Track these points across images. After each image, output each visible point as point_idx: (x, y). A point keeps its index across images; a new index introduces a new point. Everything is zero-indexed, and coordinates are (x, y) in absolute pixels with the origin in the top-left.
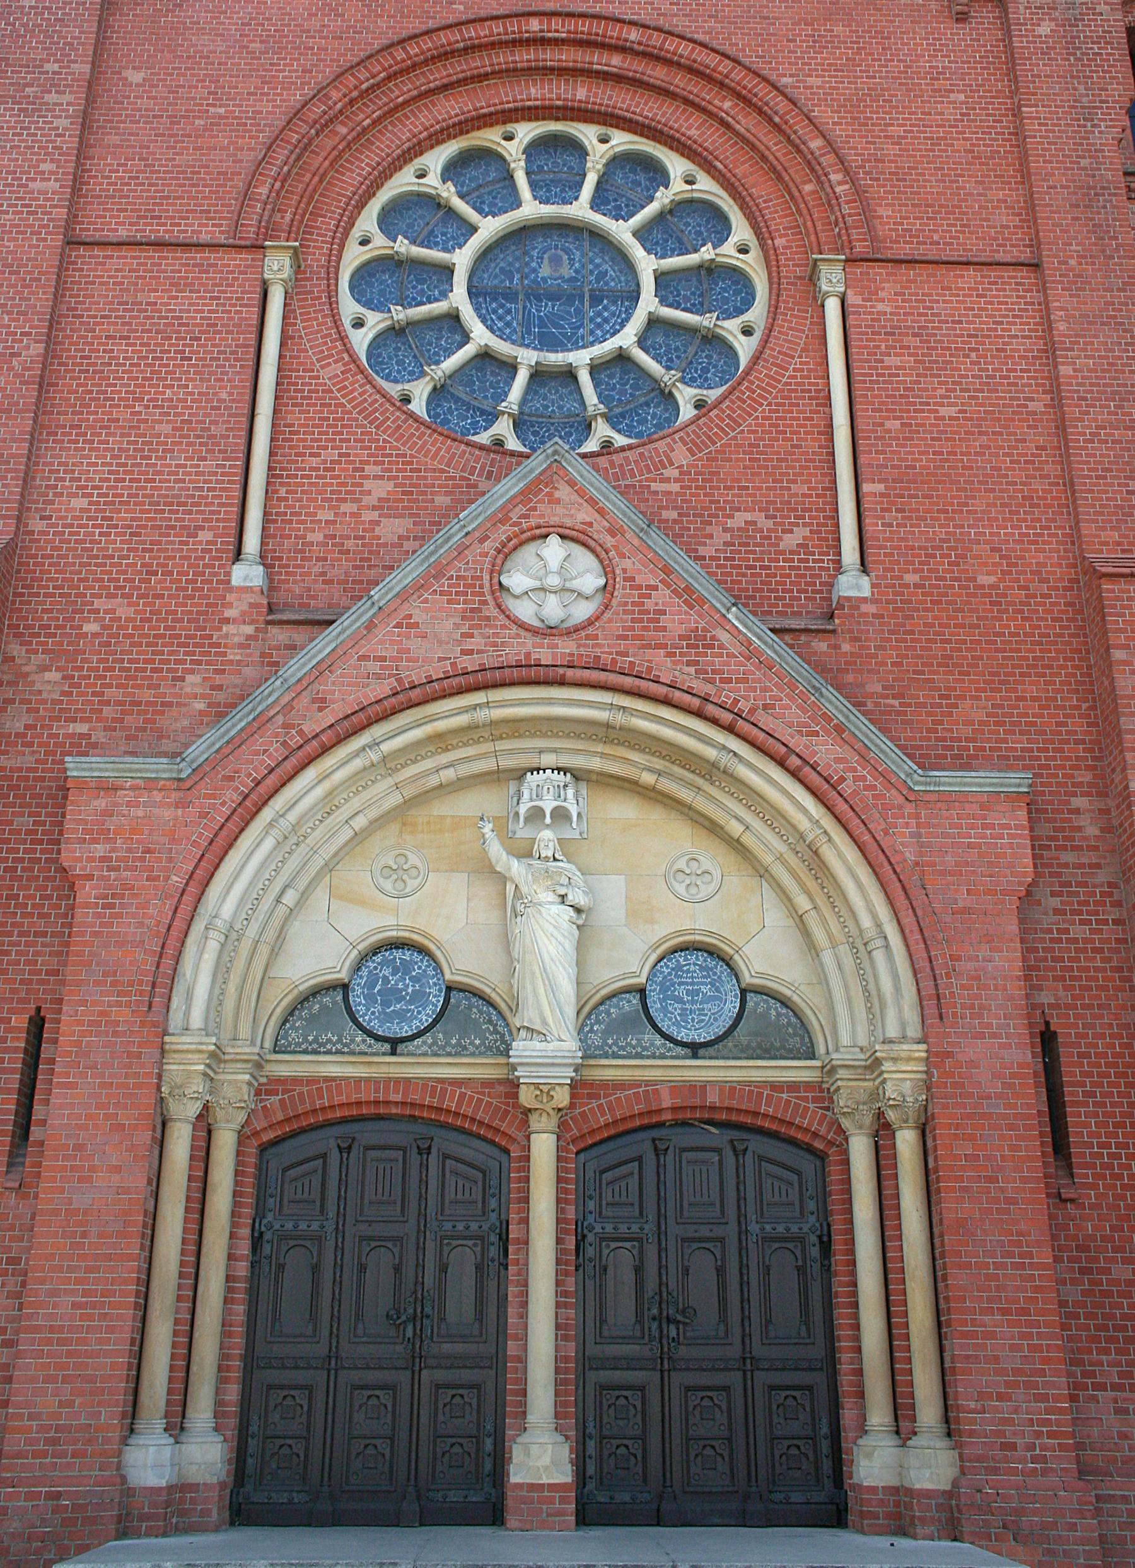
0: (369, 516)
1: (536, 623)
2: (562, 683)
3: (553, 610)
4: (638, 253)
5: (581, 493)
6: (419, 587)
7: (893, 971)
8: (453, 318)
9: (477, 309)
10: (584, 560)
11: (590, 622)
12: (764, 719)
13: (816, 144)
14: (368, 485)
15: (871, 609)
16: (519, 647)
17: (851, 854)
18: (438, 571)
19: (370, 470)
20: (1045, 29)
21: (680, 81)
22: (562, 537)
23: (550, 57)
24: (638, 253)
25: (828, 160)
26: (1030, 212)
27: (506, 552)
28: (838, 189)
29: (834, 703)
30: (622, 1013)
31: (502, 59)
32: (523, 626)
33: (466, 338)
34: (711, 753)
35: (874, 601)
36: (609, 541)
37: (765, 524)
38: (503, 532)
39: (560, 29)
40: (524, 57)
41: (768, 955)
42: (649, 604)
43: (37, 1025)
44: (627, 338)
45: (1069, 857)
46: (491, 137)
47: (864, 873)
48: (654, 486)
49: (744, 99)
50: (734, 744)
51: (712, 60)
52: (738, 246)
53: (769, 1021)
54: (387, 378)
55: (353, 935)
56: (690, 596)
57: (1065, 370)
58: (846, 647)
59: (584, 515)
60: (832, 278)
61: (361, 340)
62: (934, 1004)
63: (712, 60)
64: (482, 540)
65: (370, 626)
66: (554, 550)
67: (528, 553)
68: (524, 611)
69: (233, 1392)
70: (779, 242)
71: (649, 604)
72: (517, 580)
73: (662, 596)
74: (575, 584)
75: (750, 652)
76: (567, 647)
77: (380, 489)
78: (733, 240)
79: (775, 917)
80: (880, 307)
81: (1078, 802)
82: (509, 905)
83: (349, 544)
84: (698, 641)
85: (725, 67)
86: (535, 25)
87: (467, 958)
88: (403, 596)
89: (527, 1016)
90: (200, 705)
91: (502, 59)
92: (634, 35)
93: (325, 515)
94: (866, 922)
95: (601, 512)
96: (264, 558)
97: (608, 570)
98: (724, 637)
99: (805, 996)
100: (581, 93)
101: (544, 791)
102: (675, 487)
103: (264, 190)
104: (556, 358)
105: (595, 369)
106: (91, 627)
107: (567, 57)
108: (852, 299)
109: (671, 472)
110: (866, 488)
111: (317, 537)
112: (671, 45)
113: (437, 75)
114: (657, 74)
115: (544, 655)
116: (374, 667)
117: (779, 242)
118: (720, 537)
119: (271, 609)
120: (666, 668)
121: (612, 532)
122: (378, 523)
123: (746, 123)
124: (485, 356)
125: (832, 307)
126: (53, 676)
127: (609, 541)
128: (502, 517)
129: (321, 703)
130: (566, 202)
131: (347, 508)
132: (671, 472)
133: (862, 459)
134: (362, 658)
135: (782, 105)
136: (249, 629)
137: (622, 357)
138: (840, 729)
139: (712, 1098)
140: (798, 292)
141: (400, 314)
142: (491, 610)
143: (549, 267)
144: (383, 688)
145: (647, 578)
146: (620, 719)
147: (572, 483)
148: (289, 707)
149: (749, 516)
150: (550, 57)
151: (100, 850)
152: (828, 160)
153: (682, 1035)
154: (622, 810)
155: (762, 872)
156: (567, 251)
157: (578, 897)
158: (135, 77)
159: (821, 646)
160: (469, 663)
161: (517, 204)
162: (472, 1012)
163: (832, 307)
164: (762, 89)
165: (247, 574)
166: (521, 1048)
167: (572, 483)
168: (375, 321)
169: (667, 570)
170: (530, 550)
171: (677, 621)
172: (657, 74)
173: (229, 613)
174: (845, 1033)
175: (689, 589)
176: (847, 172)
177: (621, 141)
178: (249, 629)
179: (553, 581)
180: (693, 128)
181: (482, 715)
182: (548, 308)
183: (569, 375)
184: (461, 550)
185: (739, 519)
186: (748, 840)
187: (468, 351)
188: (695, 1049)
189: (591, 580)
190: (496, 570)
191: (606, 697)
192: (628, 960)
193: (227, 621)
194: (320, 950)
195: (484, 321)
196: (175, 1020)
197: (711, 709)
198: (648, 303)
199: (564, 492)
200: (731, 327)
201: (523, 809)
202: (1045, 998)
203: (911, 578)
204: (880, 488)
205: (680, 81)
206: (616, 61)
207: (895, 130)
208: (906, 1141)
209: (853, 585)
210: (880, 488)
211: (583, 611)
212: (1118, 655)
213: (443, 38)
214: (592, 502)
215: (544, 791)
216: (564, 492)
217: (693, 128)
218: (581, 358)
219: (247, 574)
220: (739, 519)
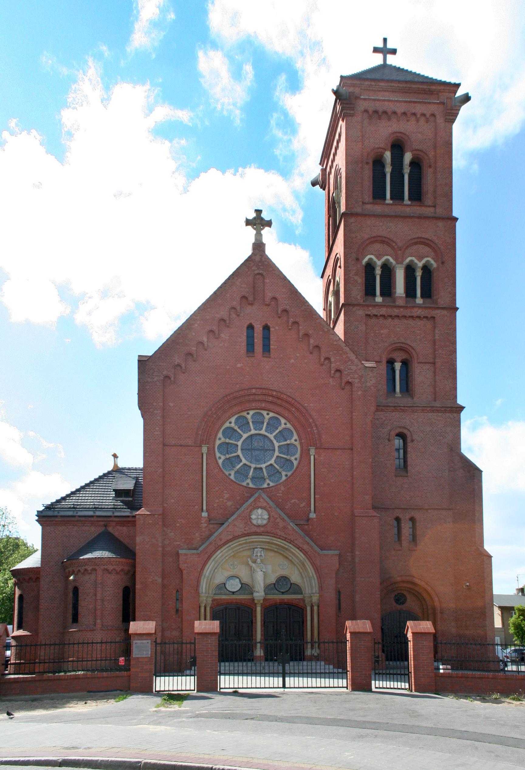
1: (256, 524)
3: (260, 522)
4: (275, 442)
5: (265, 500)
6: (236, 519)
8: (238, 456)
9: (244, 455)
10: (265, 513)
11: (266, 524)
12: (295, 541)
13: (311, 421)
18: (239, 516)
20: (359, 393)
21: (284, 404)
23: (257, 398)
24: (275, 442)
26: (352, 437)
28: (315, 431)
29: (307, 539)
32: (254, 525)
33: (241, 461)
34: (286, 547)
35: (316, 518)
36: (270, 509)
42: (276, 521)
44: (272, 461)
46: (245, 414)
48: (278, 495)
52: (294, 439)
56: (283, 520)
57: (355, 473)
58: (310, 527)
59: (265, 504)
60: (312, 452)
61: (220, 462)
65: (228, 526)
66: (260, 511)
67: (255, 512)
68: (254, 522)
71: (276, 521)
73: (278, 520)
74: (264, 517)
75: (294, 530)
76: (262, 529)
78: (294, 438)
80: (322, 458)
84: (285, 528)
86: (254, 391)
88: (234, 520)
90: (199, 539)
93: (217, 501)
95: (268, 504)
97: (269, 515)
98: (289, 527)
103: (200, 432)
104: (258, 466)
107: (260, 397)
108: (316, 457)
109: (280, 492)
110: (316, 496)
111: (215, 505)
114: (279, 402)
115: (258, 530)
116: (229, 533)
118: (289, 505)
119: (209, 521)
120: (280, 533)
121: (270, 508)
123: (297, 414)
125: (312, 457)
127: (270, 509)
128: (251, 505)
129: (221, 540)
130: (260, 430)
131: (221, 499)
132: (280, 492)
137: (271, 465)
138: (308, 543)
141: (228, 456)
142: (249, 523)
148: (215, 541)
156: (260, 439)
159: (306, 527)
163: (312, 457)
164: (301, 407)
165: (205, 514)
167: (263, 498)
168: (223, 458)
169: (280, 515)
170: (256, 510)
171: (281, 524)
173: (202, 522)
175: (283, 518)
176: (317, 427)
177: (271, 414)
178: (206, 525)
181: (248, 541)
184: (243, 511)
187: (241, 464)
189: (266, 517)
190: (250, 515)
199: (261, 500)
200: (293, 458)
203: (323, 514)
207: (327, 417)
209: (312, 515)
211: (265, 522)
214: (267, 502)
216: (261, 500)
218: (263, 466)
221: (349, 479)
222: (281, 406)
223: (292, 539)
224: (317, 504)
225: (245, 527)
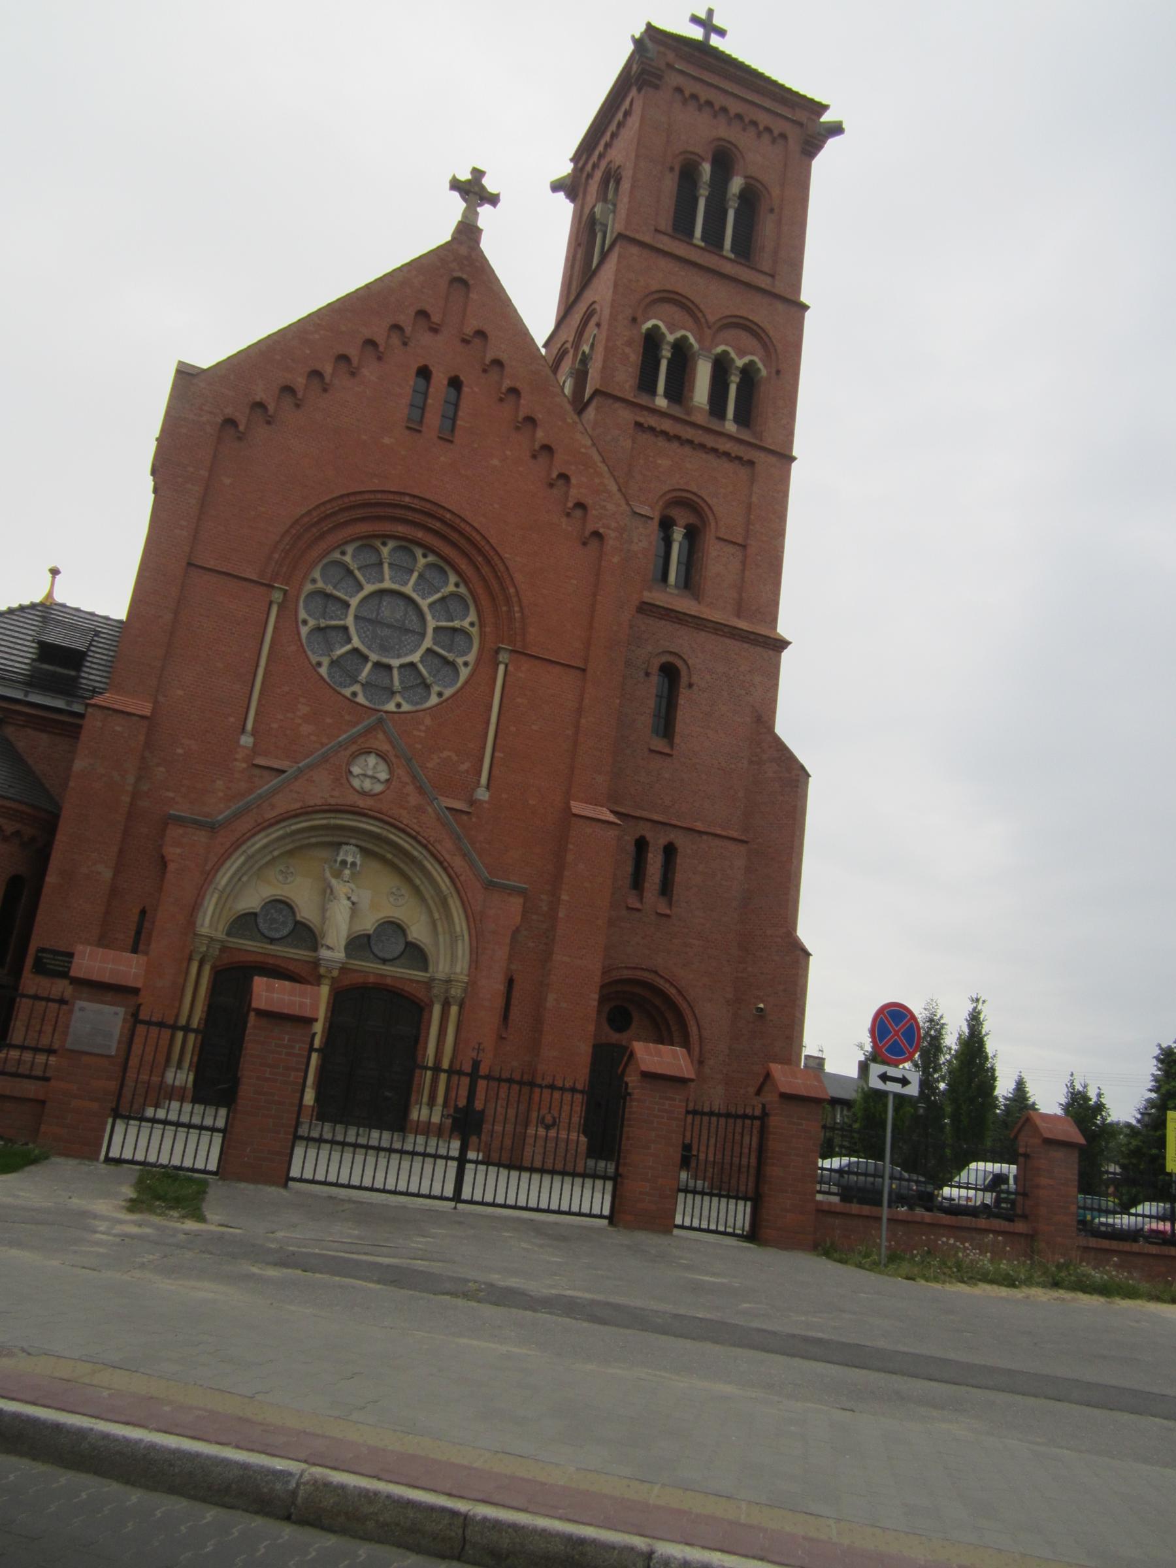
0: (300, 721)
2: (365, 815)
3: (367, 785)
7: (463, 950)
10: (382, 766)
11: (382, 793)
14: (300, 706)
15: (486, 806)
16: (353, 799)
17: (458, 903)
19: (302, 700)
21: (462, 542)
22: (377, 755)
23: (411, 516)
25: (515, 599)
27: (354, 756)
30: (359, 944)
31: (390, 511)
32: (354, 789)
36: (394, 760)
37: (455, 758)
38: (354, 748)
39: (417, 504)
40: (399, 512)
41: (418, 932)
43: (143, 912)
45: (534, 917)
47: (461, 911)
49: (489, 562)
50: (424, 852)
51: (478, 538)
53: (416, 954)
54: (312, 650)
55: (264, 896)
57: (583, 721)
60: (503, 657)
62: (475, 963)
63: (478, 538)
64: (346, 749)
66: (372, 760)
68: (356, 783)
69: (195, 1059)
70: (488, 629)
72: (356, 770)
73: (410, 788)
77: (304, 709)
79: (424, 918)
81: (543, 897)
82: (327, 893)
83: (288, 732)
85: (483, 543)
86: (407, 499)
87: (307, 911)
89: (329, 941)
91: (390, 511)
92: (448, 516)
94: (458, 929)
96: (254, 733)
97: (391, 772)
98: (430, 810)
99: (429, 949)
100: (420, 534)
101: (349, 854)
102: (423, 734)
105: (402, 666)
106: (180, 751)
108: (510, 668)
110: (497, 754)
112: (463, 525)
113: (359, 513)
114: (455, 536)
117: (488, 629)
122: (300, 725)
123: (485, 570)
124: (356, 651)
126: (162, 769)
127: (394, 760)
128: (353, 740)
133: (498, 741)
134: (291, 791)
135: (502, 568)
136: (244, 765)
139: (389, 981)
140: (489, 659)
142: (344, 781)
143: (390, 611)
144: (297, 805)
145: (406, 779)
146: (385, 833)
147: (385, 732)
149: (449, 754)
150: (411, 516)
151: (178, 851)
152: (515, 599)
153: (380, 954)
154: (375, 865)
155: (423, 899)
157: (354, 899)
158: (227, 481)
160: (333, 801)
161: (382, 580)
162: (306, 935)
166: (324, 953)
172: (455, 536)
174: (441, 967)
179: (370, 773)
180: (463, 565)
182: (387, 632)
183: (389, 668)
185: (445, 754)
186: (422, 888)
188: (384, 961)
190: (349, 764)
191: (381, 825)
192: (368, 924)
193: (236, 760)
194: (252, 900)
195: (359, 637)
196: (199, 922)
197: (420, 838)
198: (428, 643)
199: (381, 736)
201: (339, 859)
202: (513, 967)
203: (504, 796)
204: (501, 755)
205: (462, 542)
206: (437, 525)
208: (454, 1010)
209: (482, 794)
210: (501, 755)
211: (378, 788)
212: (571, 846)
213: (366, 496)
215: (349, 854)
217: (463, 565)
219: (246, 740)
220: (445, 754)
221: (569, 732)
222: (454, 545)
223: (432, 839)
224: (496, 772)
225: (333, 789)
